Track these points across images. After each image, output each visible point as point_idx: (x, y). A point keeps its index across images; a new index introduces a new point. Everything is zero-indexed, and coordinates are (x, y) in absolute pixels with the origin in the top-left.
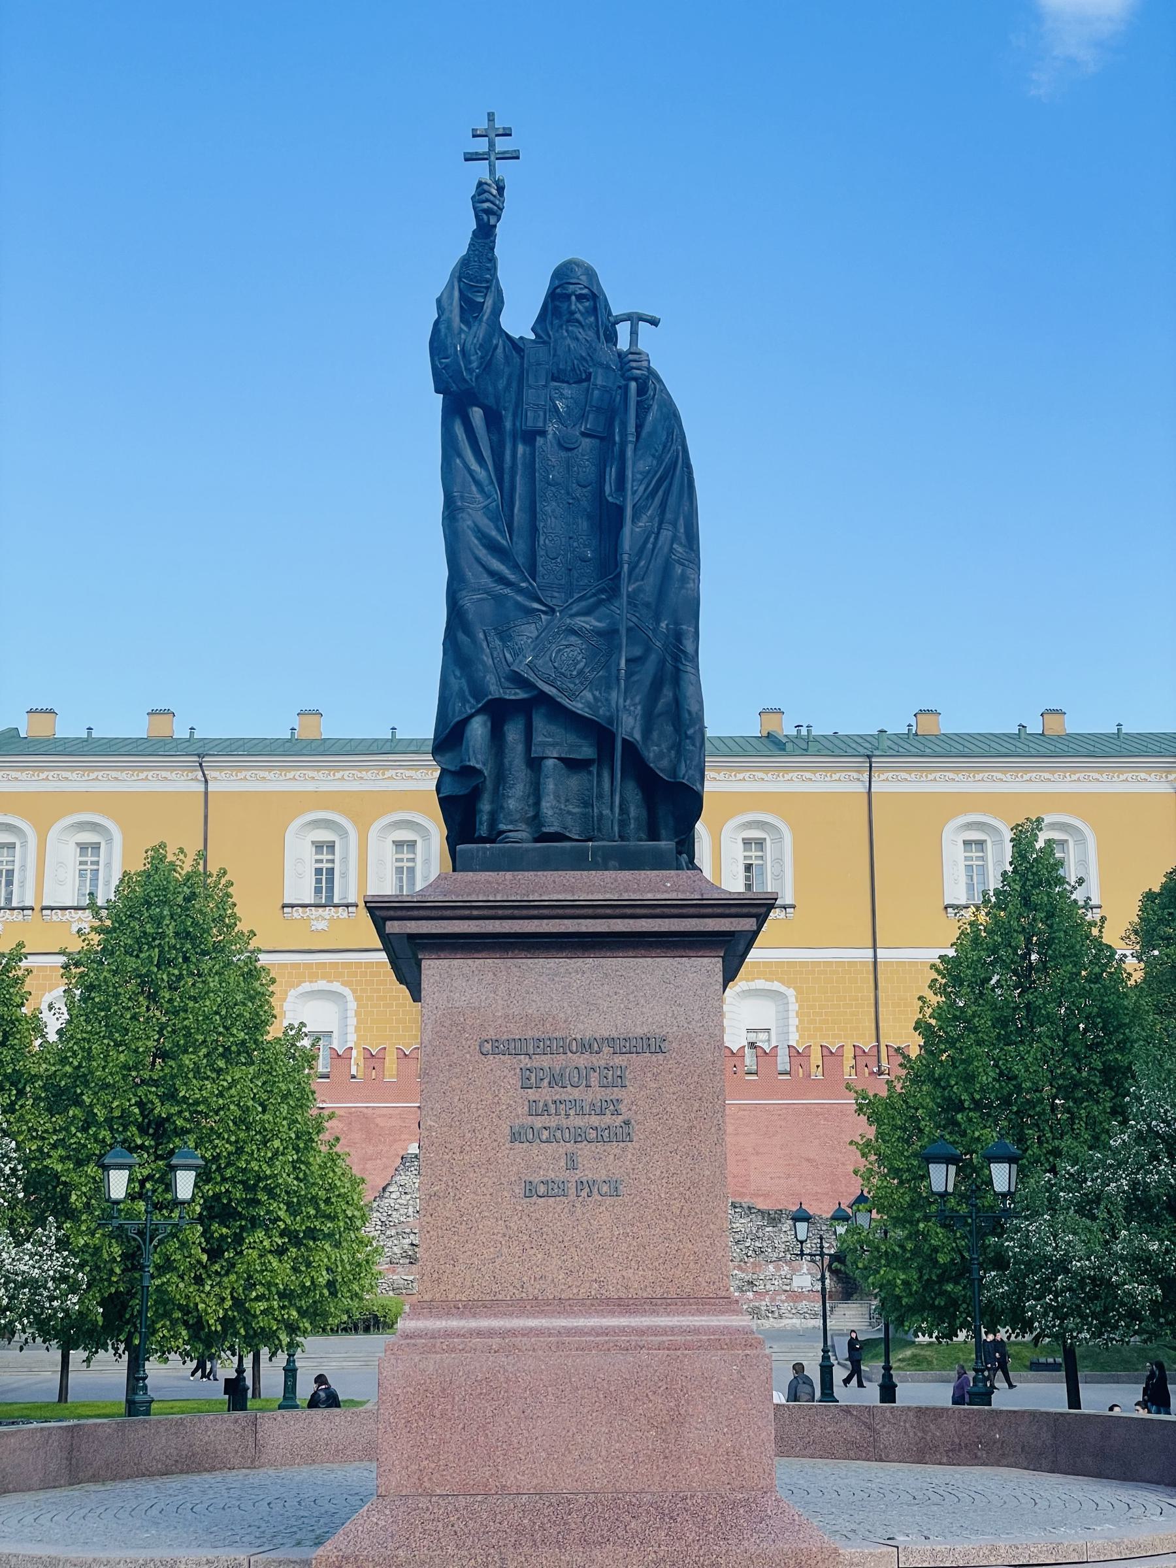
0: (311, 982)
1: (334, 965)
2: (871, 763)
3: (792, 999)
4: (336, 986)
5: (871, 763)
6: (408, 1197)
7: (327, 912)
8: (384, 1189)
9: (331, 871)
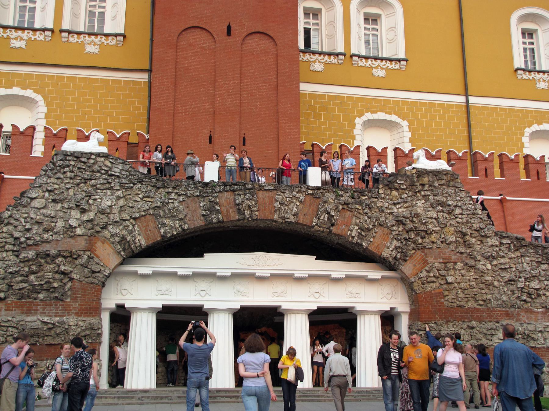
0: (6, 88)
3: (406, 129)
4: (29, 93)
6: (59, 206)
7: (25, 35)
8: (23, 194)
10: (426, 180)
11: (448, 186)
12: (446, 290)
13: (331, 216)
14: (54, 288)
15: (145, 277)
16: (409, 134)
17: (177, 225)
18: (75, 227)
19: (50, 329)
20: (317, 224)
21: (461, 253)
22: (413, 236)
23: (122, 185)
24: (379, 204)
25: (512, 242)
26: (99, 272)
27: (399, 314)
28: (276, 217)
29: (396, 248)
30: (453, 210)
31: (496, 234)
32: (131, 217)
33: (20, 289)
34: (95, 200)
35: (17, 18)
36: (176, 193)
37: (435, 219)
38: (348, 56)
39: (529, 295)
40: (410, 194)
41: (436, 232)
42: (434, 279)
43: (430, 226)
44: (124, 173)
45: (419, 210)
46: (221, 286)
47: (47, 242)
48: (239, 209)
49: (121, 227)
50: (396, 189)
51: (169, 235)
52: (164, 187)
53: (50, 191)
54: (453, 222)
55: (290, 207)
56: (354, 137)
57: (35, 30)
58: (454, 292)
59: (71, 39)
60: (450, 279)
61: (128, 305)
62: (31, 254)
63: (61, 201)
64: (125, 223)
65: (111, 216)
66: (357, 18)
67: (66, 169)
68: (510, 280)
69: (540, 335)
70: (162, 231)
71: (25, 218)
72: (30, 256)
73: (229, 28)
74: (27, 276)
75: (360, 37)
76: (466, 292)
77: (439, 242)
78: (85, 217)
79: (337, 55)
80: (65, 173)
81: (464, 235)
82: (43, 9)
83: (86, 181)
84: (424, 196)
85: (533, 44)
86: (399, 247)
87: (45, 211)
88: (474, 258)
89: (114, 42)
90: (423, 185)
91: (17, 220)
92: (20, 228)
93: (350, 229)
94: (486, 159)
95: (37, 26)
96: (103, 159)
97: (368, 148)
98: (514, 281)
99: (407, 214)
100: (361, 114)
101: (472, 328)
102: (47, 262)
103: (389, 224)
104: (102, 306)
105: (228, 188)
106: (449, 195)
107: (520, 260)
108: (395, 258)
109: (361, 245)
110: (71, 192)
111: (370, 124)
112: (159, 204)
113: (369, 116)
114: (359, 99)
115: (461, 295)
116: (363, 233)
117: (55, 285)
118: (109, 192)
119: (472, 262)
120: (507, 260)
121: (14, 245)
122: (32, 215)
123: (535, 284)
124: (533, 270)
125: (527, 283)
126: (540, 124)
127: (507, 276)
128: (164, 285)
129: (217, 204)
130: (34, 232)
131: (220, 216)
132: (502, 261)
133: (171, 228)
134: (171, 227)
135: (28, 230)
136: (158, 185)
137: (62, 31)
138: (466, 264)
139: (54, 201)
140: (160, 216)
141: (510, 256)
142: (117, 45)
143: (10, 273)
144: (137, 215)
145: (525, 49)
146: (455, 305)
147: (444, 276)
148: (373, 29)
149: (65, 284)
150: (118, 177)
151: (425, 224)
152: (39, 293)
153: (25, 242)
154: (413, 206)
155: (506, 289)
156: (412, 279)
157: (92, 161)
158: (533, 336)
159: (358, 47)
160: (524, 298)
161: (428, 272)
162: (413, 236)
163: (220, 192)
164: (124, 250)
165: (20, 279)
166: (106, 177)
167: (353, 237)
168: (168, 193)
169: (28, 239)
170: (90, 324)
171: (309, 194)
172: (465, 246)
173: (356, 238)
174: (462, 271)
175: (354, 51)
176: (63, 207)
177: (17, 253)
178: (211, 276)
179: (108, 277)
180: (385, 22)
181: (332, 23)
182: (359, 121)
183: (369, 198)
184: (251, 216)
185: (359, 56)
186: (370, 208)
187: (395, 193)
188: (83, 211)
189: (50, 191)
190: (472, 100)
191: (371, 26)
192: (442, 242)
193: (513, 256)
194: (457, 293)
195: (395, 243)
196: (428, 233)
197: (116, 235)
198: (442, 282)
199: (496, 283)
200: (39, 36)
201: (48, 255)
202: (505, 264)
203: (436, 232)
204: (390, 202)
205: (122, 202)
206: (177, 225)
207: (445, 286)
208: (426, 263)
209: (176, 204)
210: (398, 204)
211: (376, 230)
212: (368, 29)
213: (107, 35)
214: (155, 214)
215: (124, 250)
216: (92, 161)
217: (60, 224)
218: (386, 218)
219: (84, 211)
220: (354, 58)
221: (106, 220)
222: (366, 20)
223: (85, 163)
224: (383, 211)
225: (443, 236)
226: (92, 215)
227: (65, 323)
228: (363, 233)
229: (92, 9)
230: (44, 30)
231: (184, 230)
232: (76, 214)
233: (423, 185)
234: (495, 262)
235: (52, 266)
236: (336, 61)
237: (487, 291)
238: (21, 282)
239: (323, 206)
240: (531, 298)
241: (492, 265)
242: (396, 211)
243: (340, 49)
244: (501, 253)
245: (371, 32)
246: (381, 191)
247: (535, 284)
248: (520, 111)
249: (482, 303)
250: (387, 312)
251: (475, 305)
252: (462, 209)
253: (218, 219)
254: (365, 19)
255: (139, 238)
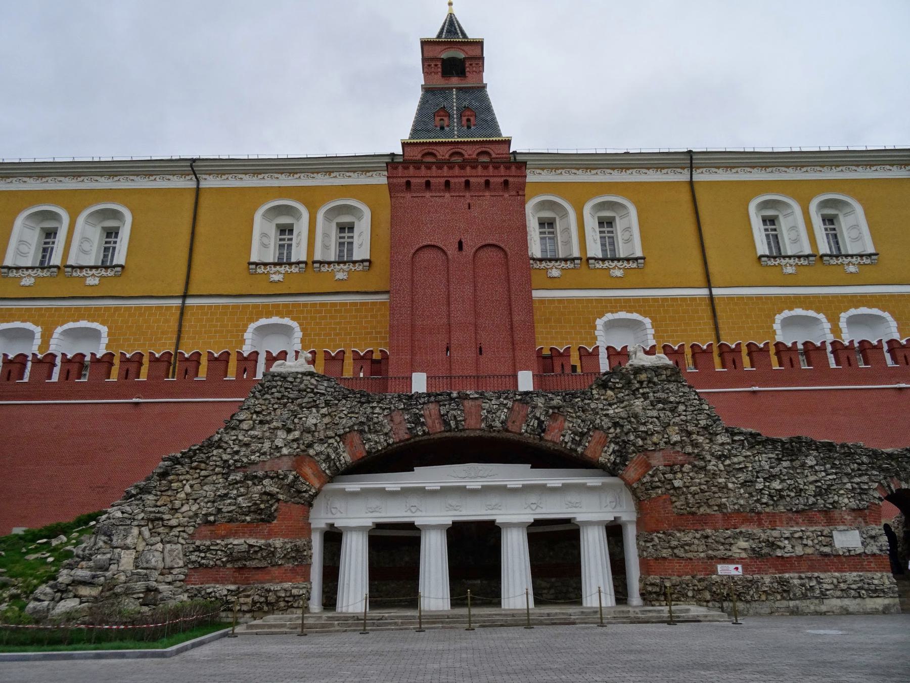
1: (286, 306)
2: (691, 159)
3: (649, 326)
4: (287, 321)
5: (691, 159)
7: (282, 269)
9: (290, 246)
10: (643, 377)
11: (669, 381)
12: (673, 495)
13: (541, 423)
14: (261, 509)
15: (354, 494)
16: (653, 331)
17: (382, 440)
18: (281, 447)
19: (256, 552)
20: (526, 431)
21: (689, 454)
22: (632, 438)
23: (327, 404)
24: (593, 406)
25: (746, 439)
26: (305, 492)
27: (625, 523)
28: (483, 425)
29: (614, 452)
30: (676, 407)
31: (727, 431)
32: (336, 434)
33: (228, 512)
34: (301, 418)
35: (277, 255)
36: (381, 408)
37: (656, 418)
38: (584, 259)
39: (771, 496)
40: (627, 392)
41: (658, 432)
42: (659, 484)
43: (651, 427)
44: (329, 389)
45: (638, 410)
46: (434, 501)
47: (253, 463)
48: (444, 420)
49: (326, 445)
50: (611, 389)
51: (373, 451)
52: (369, 402)
53: (258, 413)
54: (677, 420)
55: (498, 414)
56: (596, 338)
57: (291, 264)
58: (682, 497)
59: (323, 269)
60: (677, 483)
61: (338, 523)
62: (239, 476)
63: (268, 422)
64: (330, 441)
65: (316, 434)
66: (591, 223)
67: (274, 390)
68: (746, 482)
69: (786, 542)
70: (367, 446)
71: (234, 440)
72: (238, 478)
73: (460, 244)
74: (235, 499)
75: (595, 241)
76: (697, 496)
77: (662, 443)
78: (291, 437)
79: (573, 259)
80: (273, 393)
81: (689, 434)
82: (298, 244)
83: (293, 400)
84: (643, 394)
85: (775, 230)
86: (618, 451)
87: (252, 433)
88: (703, 459)
89: (361, 267)
90: (641, 382)
91: (226, 443)
92: (229, 450)
93: (561, 434)
94: (733, 351)
95: (293, 260)
96: (309, 378)
97: (608, 348)
98: (751, 482)
99: (624, 415)
100: (601, 315)
101: (707, 537)
102: (254, 484)
103: (605, 427)
104: (312, 526)
105: (432, 399)
106: (671, 392)
107: (757, 458)
108: (614, 463)
109: (576, 451)
110: (278, 412)
111: (611, 326)
112: (363, 419)
113: (609, 316)
114: (599, 300)
115: (691, 501)
116: (577, 438)
117: (262, 506)
118: (314, 410)
119: (702, 463)
120: (741, 459)
121: (223, 468)
122: (241, 437)
123: (776, 485)
124: (772, 468)
125: (767, 484)
126: (791, 309)
127: (742, 477)
128: (374, 503)
129: (422, 416)
130: (242, 453)
131: (425, 428)
132: (735, 460)
133: (376, 443)
134: (378, 442)
135: (237, 452)
136: (363, 400)
137: (314, 262)
138: (694, 466)
139: (261, 422)
140: (365, 432)
141: (745, 454)
142: (363, 270)
143: (219, 496)
144: (342, 432)
145: (767, 236)
146: (685, 512)
147: (671, 480)
148: (609, 232)
149: (272, 505)
150: (323, 394)
151: (644, 424)
152: (247, 515)
153: (234, 464)
154: (632, 405)
155: (742, 491)
156: (635, 485)
157: (298, 380)
158: (779, 543)
159: (594, 250)
160: (764, 501)
161: (652, 476)
162: (632, 438)
163: (424, 403)
164: (329, 468)
165: (229, 501)
166: (312, 395)
167: (566, 443)
168: (373, 408)
169: (236, 461)
170: (295, 546)
171: (517, 400)
172: (692, 445)
173: (570, 444)
174: (691, 474)
175: (590, 254)
176: (270, 428)
177: (226, 476)
178: (421, 492)
179: (316, 494)
180: (619, 225)
181: (567, 230)
182: (599, 323)
183: (582, 401)
184: (457, 427)
185: (596, 259)
186: (583, 411)
187: (610, 393)
188: (289, 431)
189: (258, 413)
190: (715, 291)
191: (606, 229)
192: (666, 443)
193: (749, 453)
194: (686, 499)
195: (613, 445)
196: (648, 434)
197: (321, 452)
198: (668, 487)
199: (730, 485)
200: (294, 269)
201: (256, 477)
202: (739, 463)
203: (658, 432)
204: (605, 402)
205: (327, 420)
206: (382, 440)
207: (672, 491)
208: (649, 466)
209: (381, 418)
210: (614, 404)
211: (591, 433)
212: (604, 232)
213: (354, 262)
214: (361, 430)
215: (329, 468)
216: (298, 380)
217: (267, 445)
218: (602, 420)
219: (289, 431)
220: (591, 261)
221: (311, 438)
222: (601, 224)
223: (291, 382)
224: (597, 413)
225: (666, 436)
226: (297, 434)
227: (270, 546)
228: (577, 438)
229: (342, 240)
230: (298, 263)
231: (389, 444)
232: (281, 434)
233: (641, 382)
234: (727, 462)
235: (259, 487)
236: (572, 266)
237: (720, 494)
238: (230, 504)
239: (532, 412)
240: (773, 500)
241: (725, 466)
242: (611, 412)
243: (576, 253)
244: (734, 452)
245: (607, 235)
246: (594, 392)
247: (776, 485)
248: (768, 298)
249: (716, 508)
250: (611, 521)
251: (708, 511)
252: (686, 406)
253: (424, 431)
254: (599, 223)
255: (345, 455)
